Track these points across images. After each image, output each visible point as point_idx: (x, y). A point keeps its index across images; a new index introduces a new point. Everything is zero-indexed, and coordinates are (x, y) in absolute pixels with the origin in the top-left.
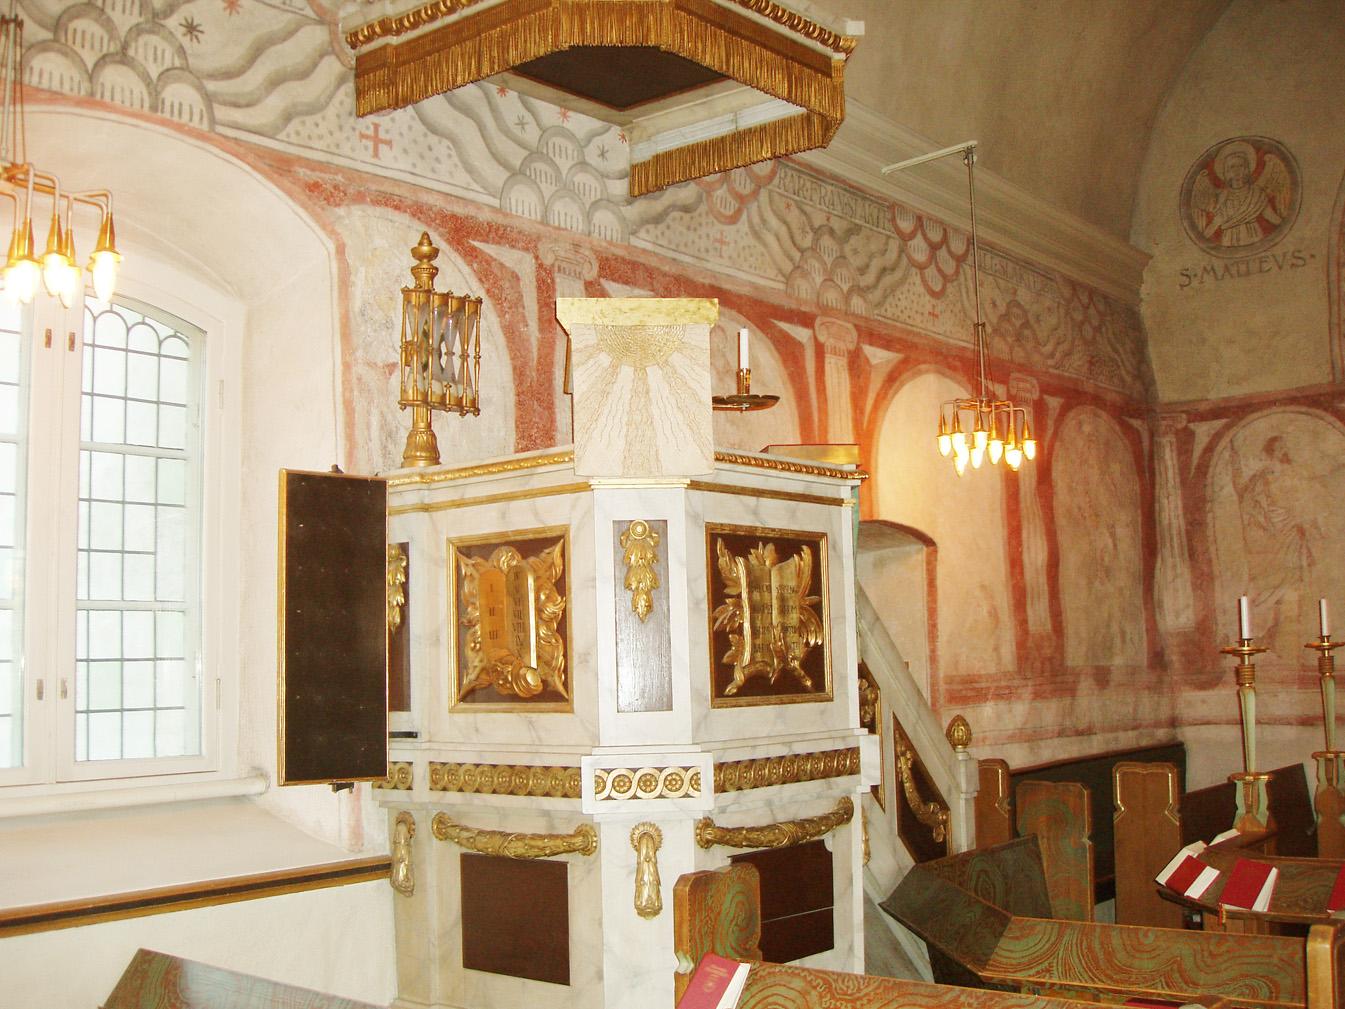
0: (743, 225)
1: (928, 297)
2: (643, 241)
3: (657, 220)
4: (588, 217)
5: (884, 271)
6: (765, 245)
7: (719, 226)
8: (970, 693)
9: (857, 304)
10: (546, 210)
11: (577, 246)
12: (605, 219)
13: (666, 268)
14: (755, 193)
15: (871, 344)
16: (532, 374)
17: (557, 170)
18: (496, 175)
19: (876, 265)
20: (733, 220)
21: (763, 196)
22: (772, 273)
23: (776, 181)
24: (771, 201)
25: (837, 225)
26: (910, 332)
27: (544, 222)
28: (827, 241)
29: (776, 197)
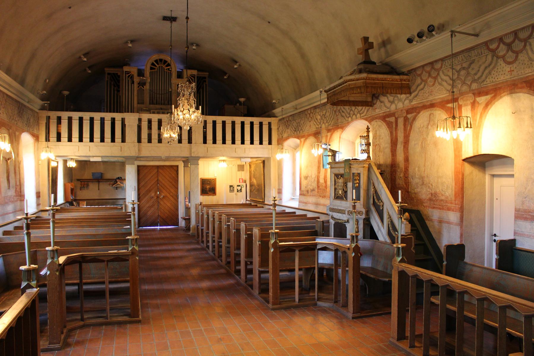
0: (437, 84)
1: (507, 66)
2: (414, 103)
3: (416, 96)
4: (403, 103)
5: (486, 68)
6: (443, 86)
7: (430, 88)
8: (528, 216)
9: (474, 86)
10: (396, 106)
11: (402, 110)
12: (407, 102)
13: (420, 105)
14: (438, 74)
15: (479, 97)
16: (394, 139)
17: (398, 97)
18: (388, 104)
19: (483, 68)
20: (434, 85)
21: (441, 73)
22: (445, 92)
23: (443, 67)
24: (443, 73)
25: (465, 65)
26: (497, 85)
27: (396, 109)
28: (463, 73)
29: (444, 71)
